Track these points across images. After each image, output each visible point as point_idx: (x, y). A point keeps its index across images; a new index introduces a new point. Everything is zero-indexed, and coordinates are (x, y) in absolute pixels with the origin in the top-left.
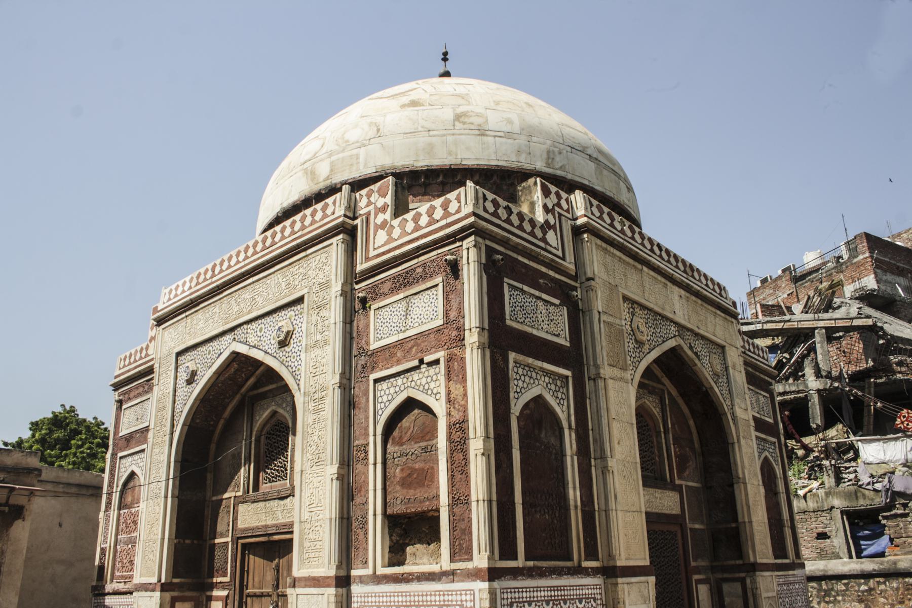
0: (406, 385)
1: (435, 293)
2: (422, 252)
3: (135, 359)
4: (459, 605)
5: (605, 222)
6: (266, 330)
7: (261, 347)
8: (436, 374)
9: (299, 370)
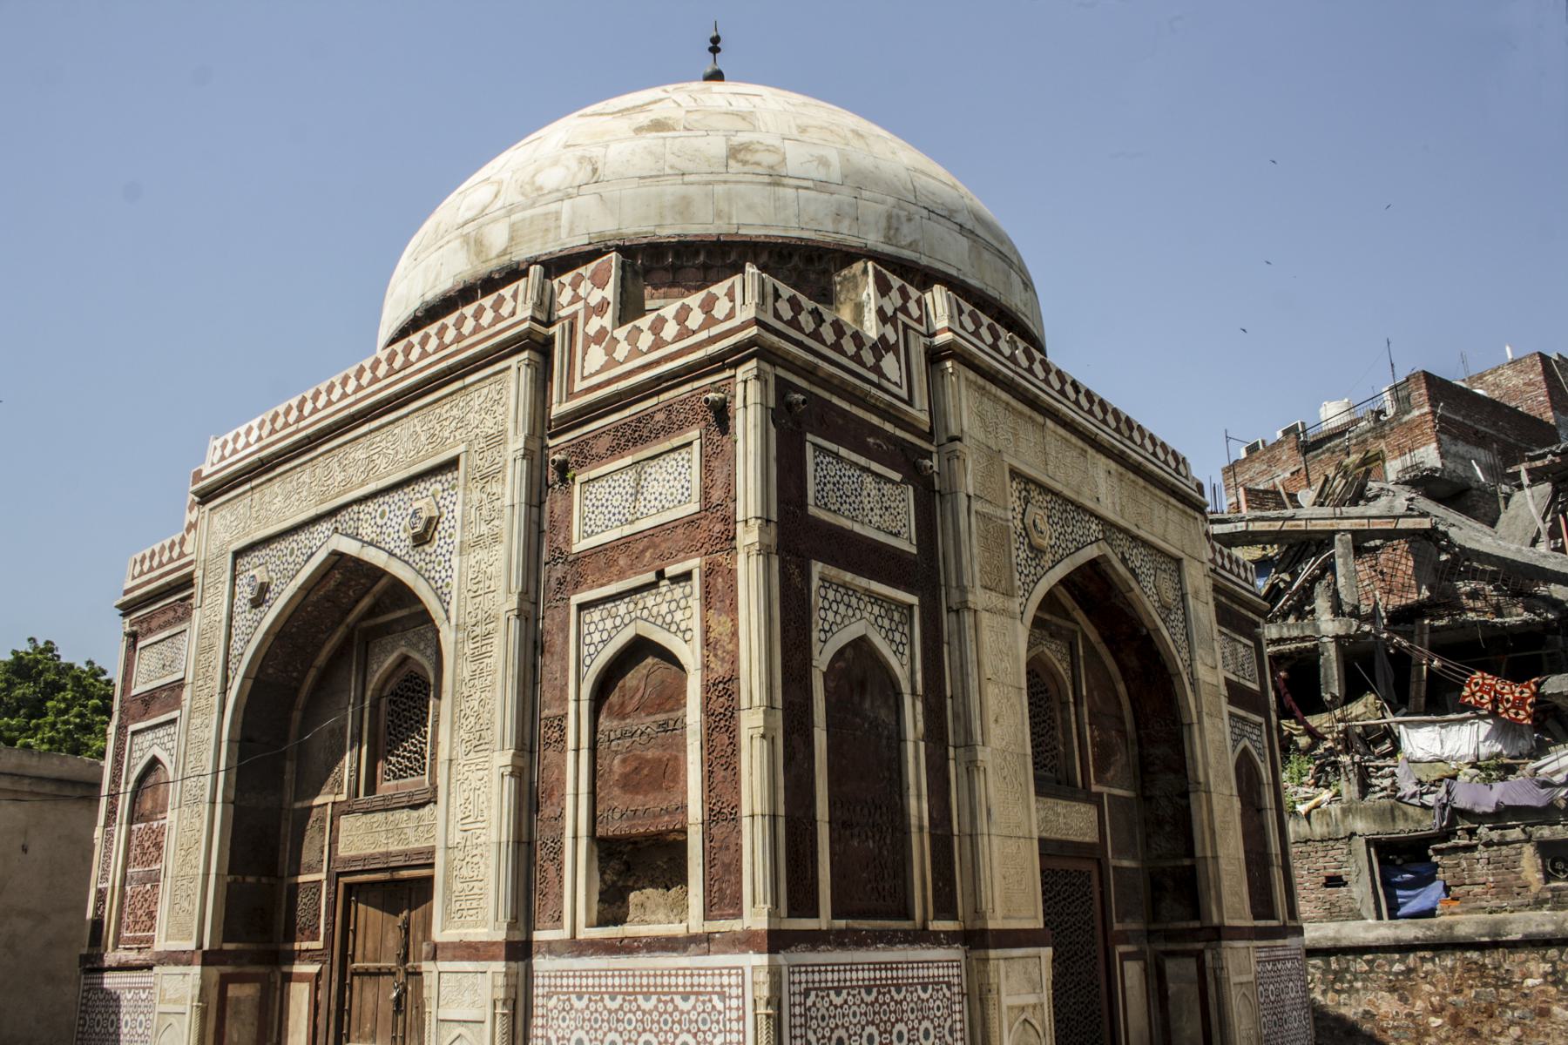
0: (633, 615)
1: (687, 457)
2: (665, 385)
3: (161, 561)
4: (716, 993)
5: (983, 341)
6: (392, 516)
7: (383, 545)
8: (686, 597)
9: (448, 585)
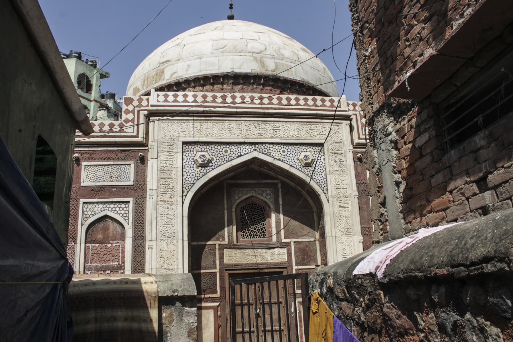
7: (286, 162)
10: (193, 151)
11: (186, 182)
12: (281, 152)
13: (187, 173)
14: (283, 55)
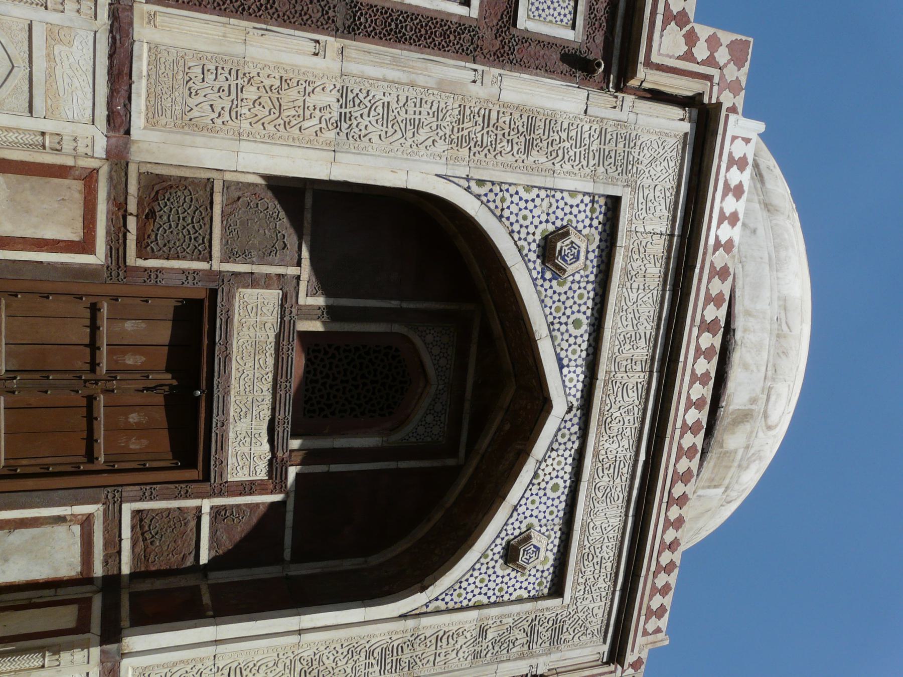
7: (528, 494)
10: (591, 226)
11: (507, 195)
12: (555, 481)
13: (533, 200)
14: (747, 467)
